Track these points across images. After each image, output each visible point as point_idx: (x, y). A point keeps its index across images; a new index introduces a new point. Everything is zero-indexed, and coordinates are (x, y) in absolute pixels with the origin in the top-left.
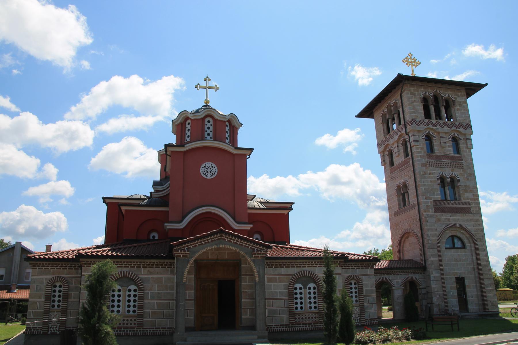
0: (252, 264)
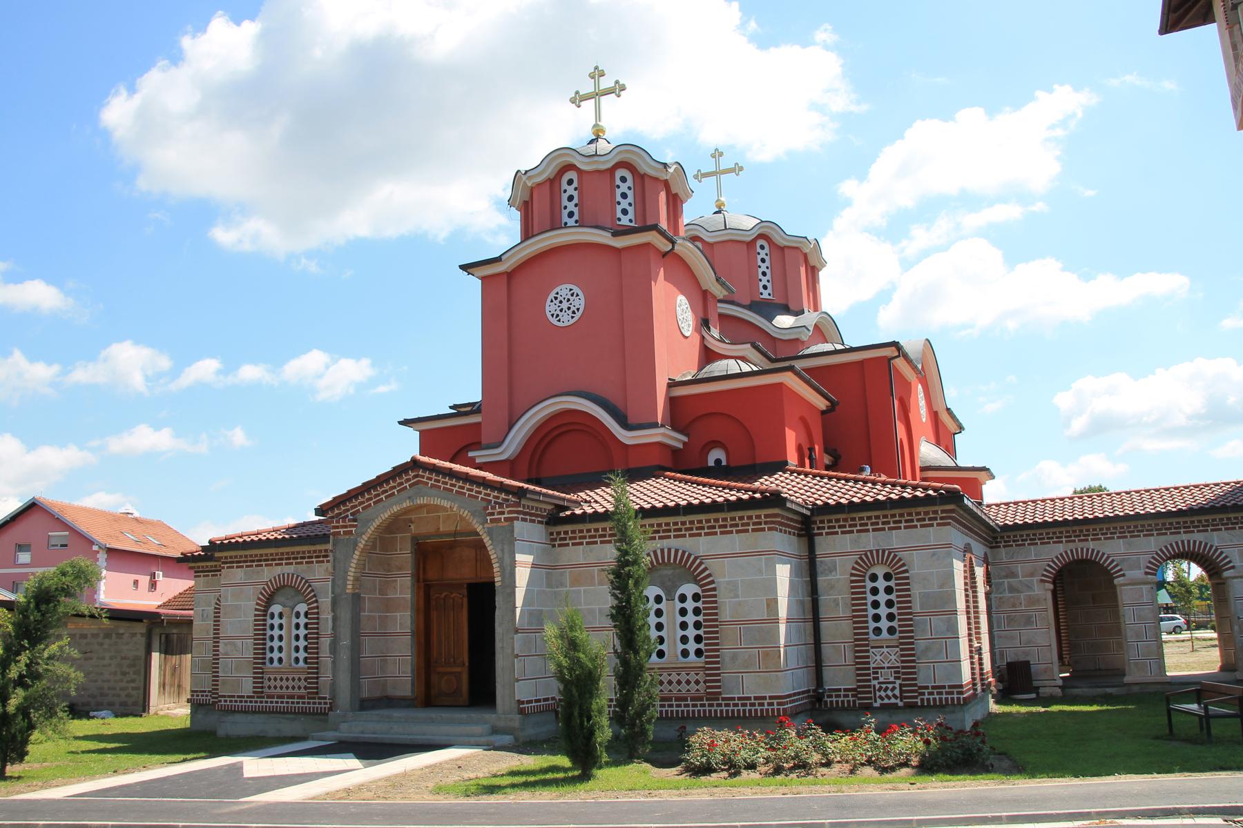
0: (486, 540)
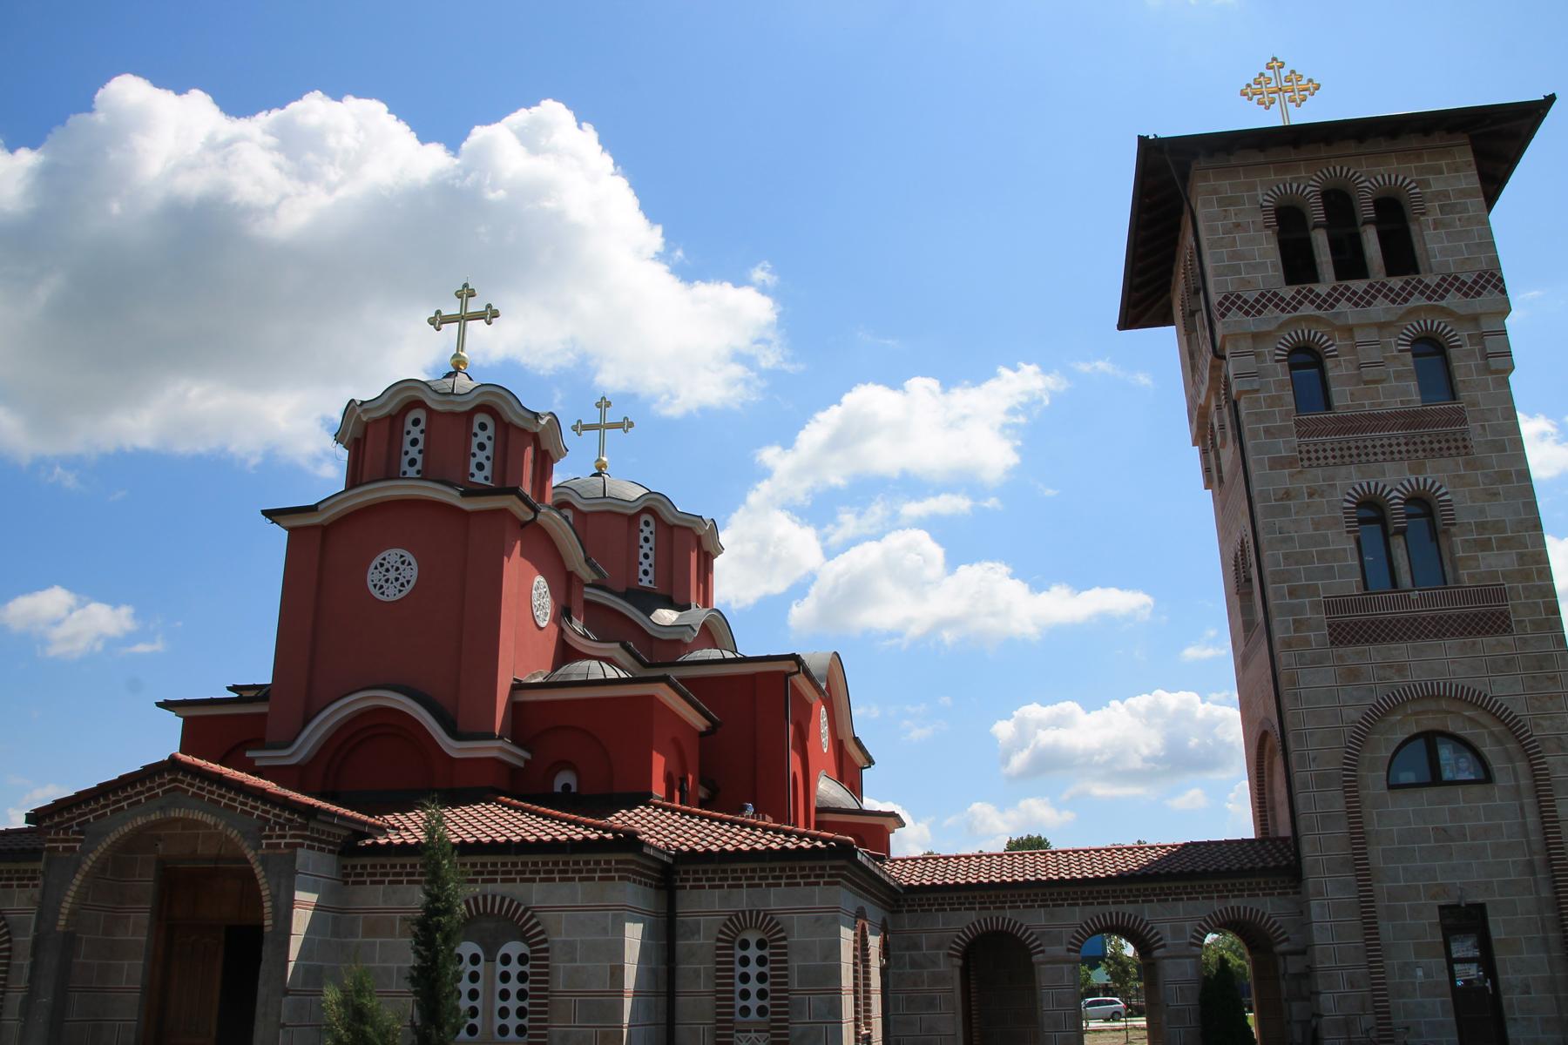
0: (258, 870)
